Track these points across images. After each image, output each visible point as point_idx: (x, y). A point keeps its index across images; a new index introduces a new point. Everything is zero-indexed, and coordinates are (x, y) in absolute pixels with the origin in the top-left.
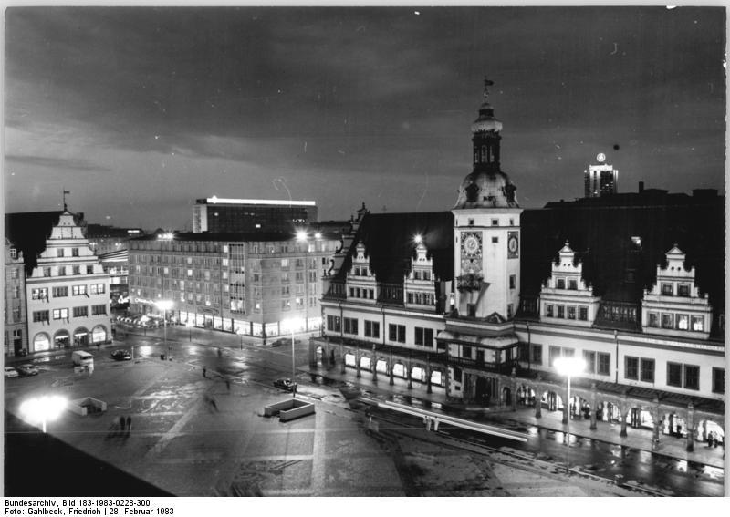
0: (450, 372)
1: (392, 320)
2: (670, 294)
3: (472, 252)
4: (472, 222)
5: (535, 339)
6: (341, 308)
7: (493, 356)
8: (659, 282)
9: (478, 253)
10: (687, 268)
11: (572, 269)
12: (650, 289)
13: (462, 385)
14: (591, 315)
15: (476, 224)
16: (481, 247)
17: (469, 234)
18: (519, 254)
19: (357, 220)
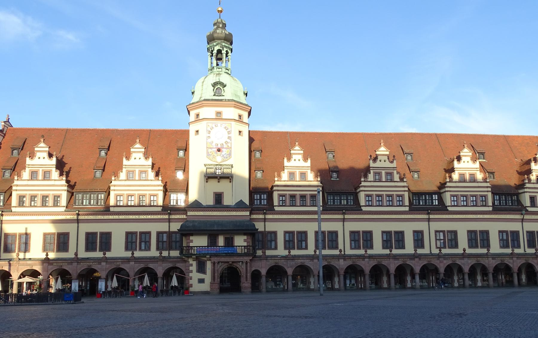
0: (192, 265)
2: (380, 181)
5: (270, 227)
7: (245, 241)
8: (372, 171)
9: (226, 143)
11: (302, 163)
13: (208, 277)
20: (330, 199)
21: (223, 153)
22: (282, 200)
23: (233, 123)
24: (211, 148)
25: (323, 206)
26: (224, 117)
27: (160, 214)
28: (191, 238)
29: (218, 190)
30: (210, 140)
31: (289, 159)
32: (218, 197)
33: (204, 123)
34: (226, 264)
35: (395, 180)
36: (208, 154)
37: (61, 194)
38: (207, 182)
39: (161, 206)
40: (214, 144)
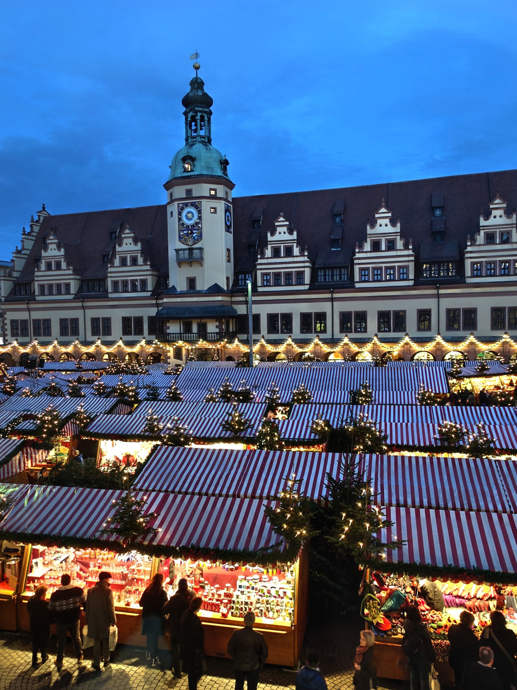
0: (169, 351)
1: (92, 313)
3: (192, 222)
4: (189, 192)
6: (29, 310)
7: (217, 327)
8: (369, 240)
9: (197, 223)
10: (393, 223)
11: (287, 237)
12: (361, 246)
14: (307, 279)
15: (194, 194)
16: (200, 218)
17: (186, 205)
18: (232, 230)
19: (37, 221)
20: (321, 276)
21: (194, 235)
22: (267, 280)
23: (204, 201)
24: (183, 231)
25: (310, 285)
26: (194, 194)
27: (150, 299)
28: (168, 325)
29: (191, 275)
30: (181, 222)
31: (273, 234)
32: (192, 282)
33: (176, 203)
34: (200, 351)
35: (398, 248)
36: (180, 238)
37: (70, 283)
38: (180, 267)
39: (150, 291)
40: (185, 226)
